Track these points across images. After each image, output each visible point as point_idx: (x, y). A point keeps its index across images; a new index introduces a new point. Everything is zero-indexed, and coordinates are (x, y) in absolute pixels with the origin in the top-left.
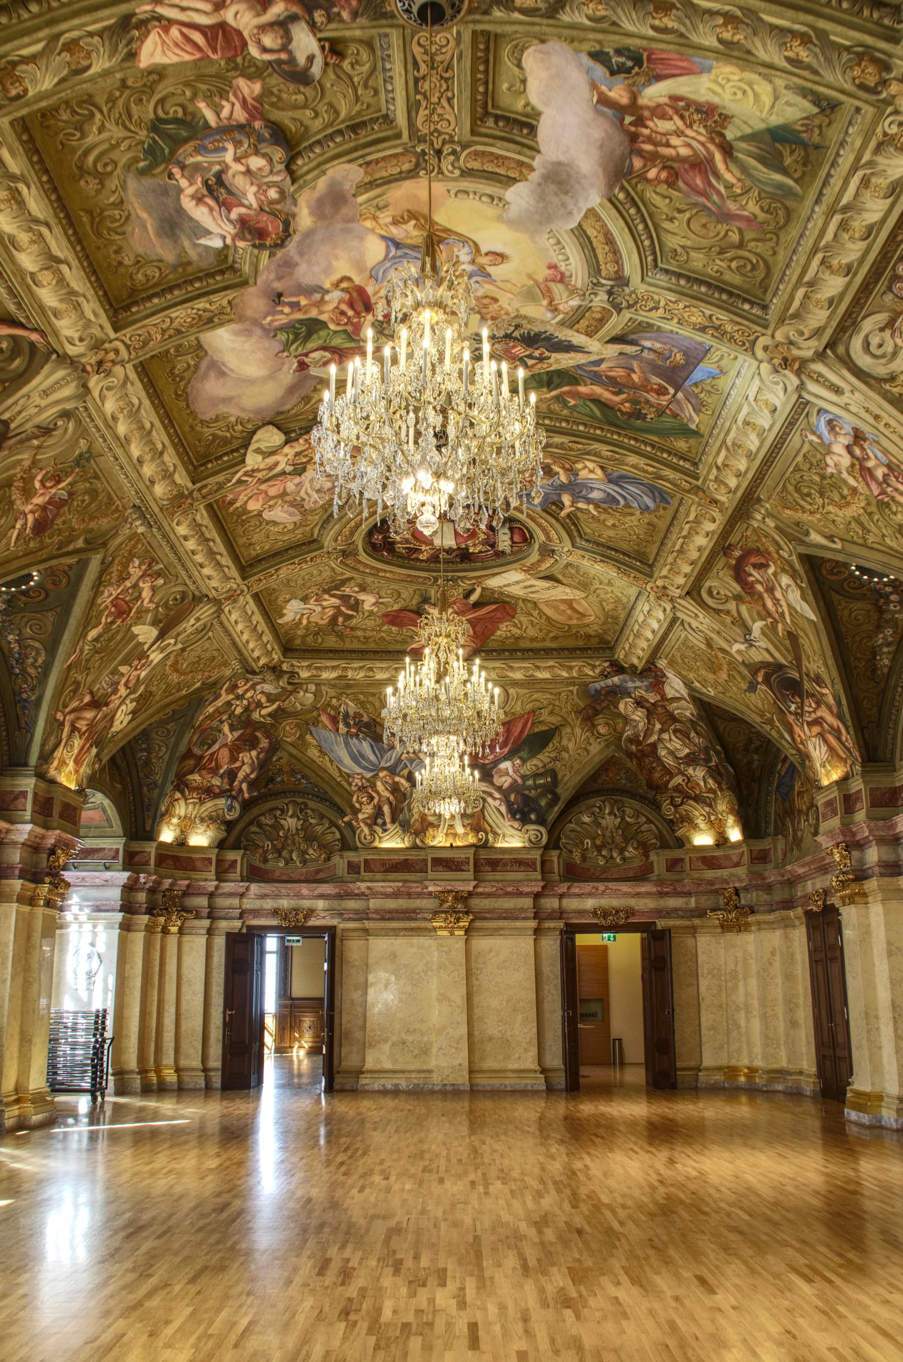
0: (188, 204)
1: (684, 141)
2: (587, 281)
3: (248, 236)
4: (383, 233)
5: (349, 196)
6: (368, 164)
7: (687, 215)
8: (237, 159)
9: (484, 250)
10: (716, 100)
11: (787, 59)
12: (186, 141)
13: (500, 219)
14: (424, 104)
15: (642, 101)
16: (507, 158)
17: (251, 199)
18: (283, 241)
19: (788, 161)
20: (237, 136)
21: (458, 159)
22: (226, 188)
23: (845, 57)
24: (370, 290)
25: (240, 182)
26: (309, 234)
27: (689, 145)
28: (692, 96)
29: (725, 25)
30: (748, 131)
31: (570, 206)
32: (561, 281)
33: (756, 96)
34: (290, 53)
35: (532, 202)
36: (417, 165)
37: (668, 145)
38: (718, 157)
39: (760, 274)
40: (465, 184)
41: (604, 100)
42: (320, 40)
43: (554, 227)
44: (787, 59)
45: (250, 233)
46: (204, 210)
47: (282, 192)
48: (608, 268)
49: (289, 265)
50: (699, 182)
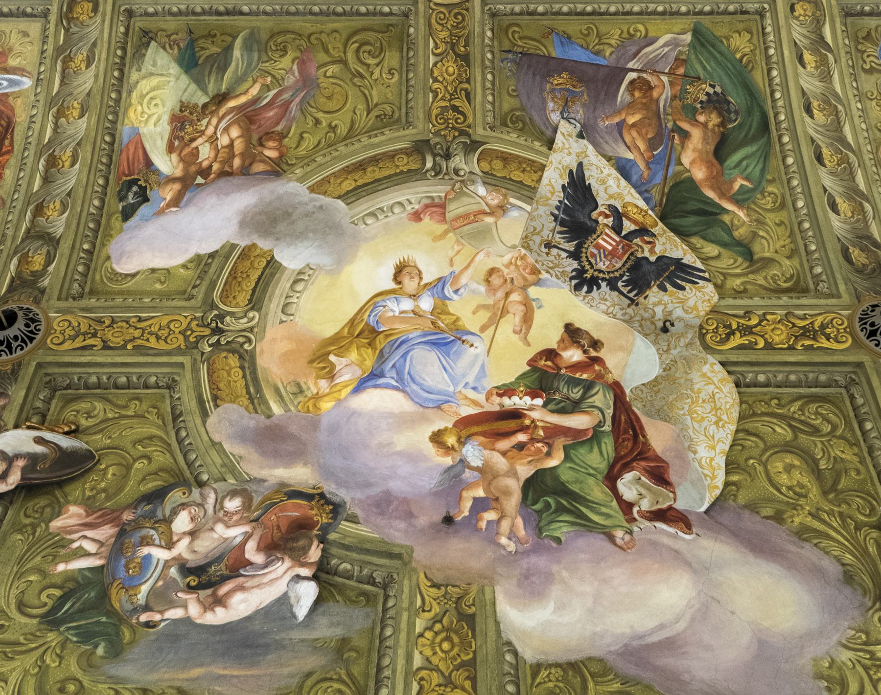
0: (219, 617)
1: (223, 134)
2: (433, 181)
3: (301, 543)
4: (349, 389)
5: (268, 422)
6: (215, 398)
7: (320, 115)
8: (170, 545)
9: (393, 285)
10: (166, 118)
11: (87, 67)
12: (104, 595)
13: (335, 272)
14: (139, 342)
15: (178, 173)
16: (234, 268)
17: (236, 533)
18: (328, 502)
19: (215, 49)
20: (135, 538)
21: (232, 314)
22: (209, 565)
23: (74, 29)
24: (467, 411)
25: (206, 545)
26: (327, 472)
27: (226, 130)
28: (166, 137)
29: (66, 117)
30: (193, 87)
31: (310, 208)
32: (443, 206)
33: (153, 89)
34: (17, 456)
35: (306, 243)
36: (233, 352)
37: (231, 145)
38: (232, 104)
39: (370, 36)
40: (274, 306)
41: (176, 202)
42: (16, 427)
43: (345, 222)
44: (87, 67)
45: (296, 539)
46: (237, 599)
47: (233, 494)
48: (404, 163)
49: (385, 504)
50: (271, 113)
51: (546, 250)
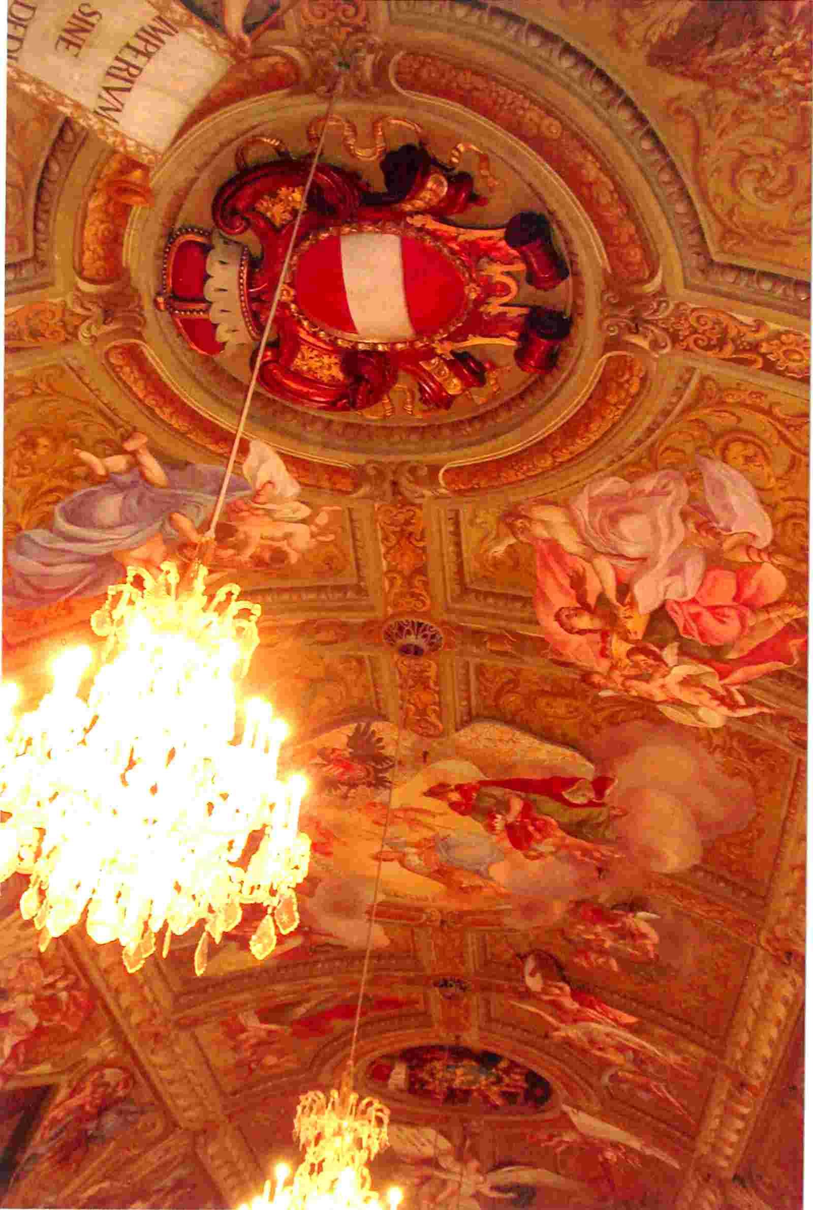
24: (507, 844)
26: (557, 897)
51: (350, 800)
